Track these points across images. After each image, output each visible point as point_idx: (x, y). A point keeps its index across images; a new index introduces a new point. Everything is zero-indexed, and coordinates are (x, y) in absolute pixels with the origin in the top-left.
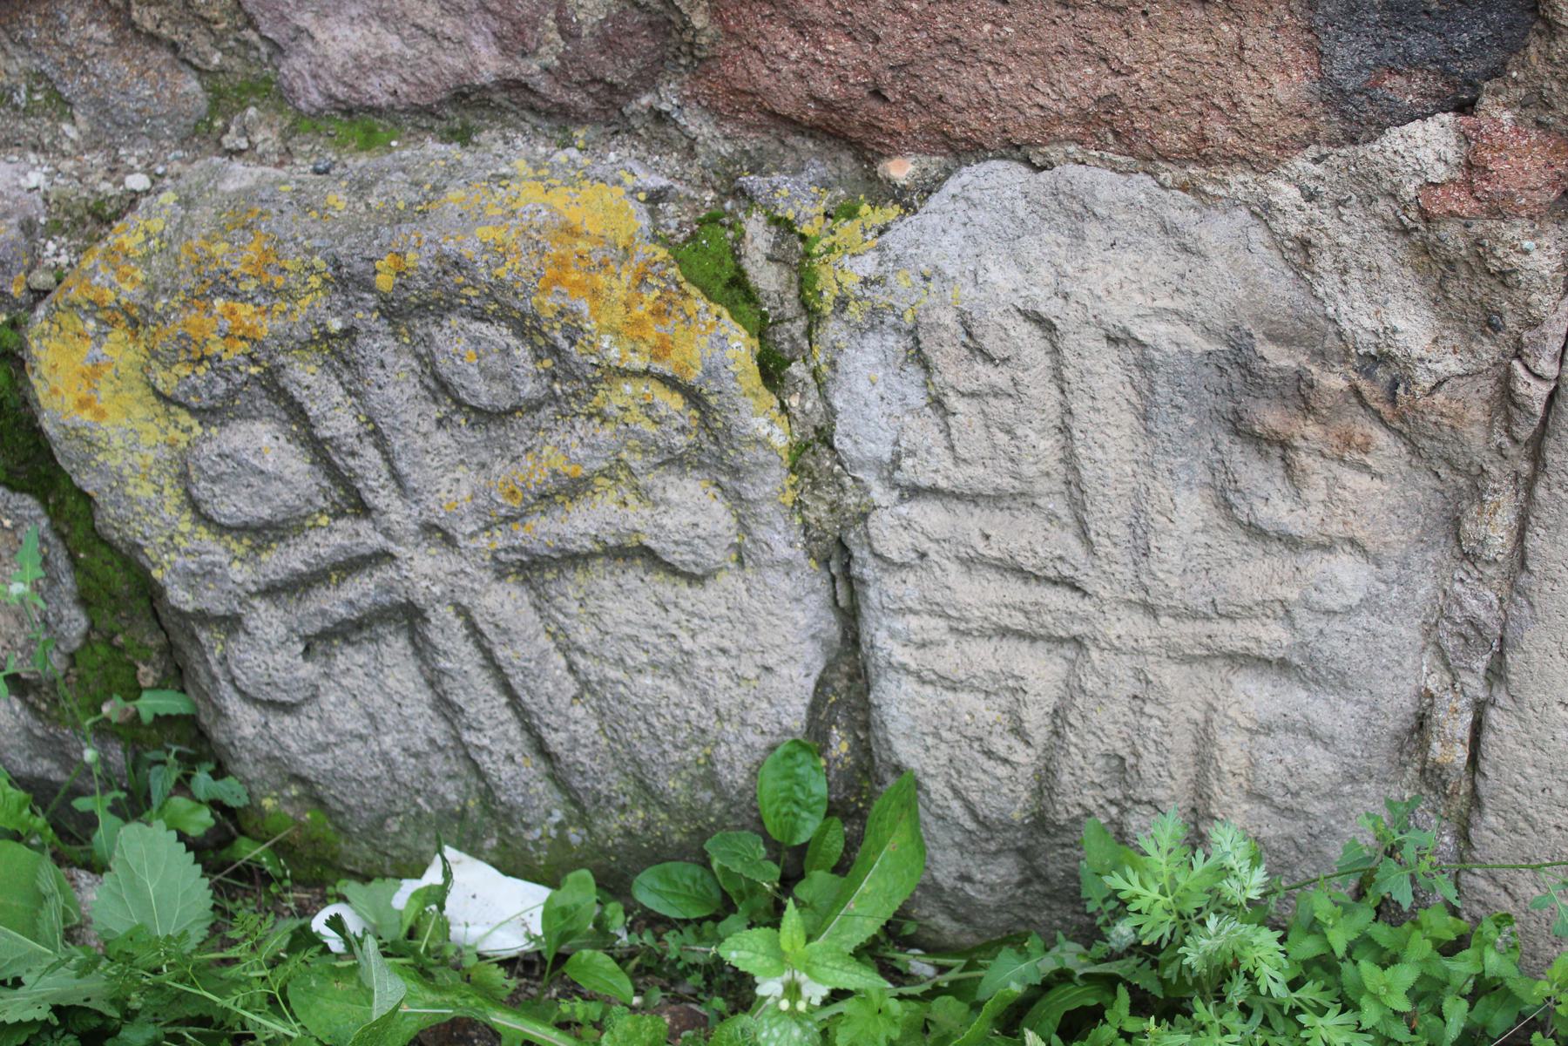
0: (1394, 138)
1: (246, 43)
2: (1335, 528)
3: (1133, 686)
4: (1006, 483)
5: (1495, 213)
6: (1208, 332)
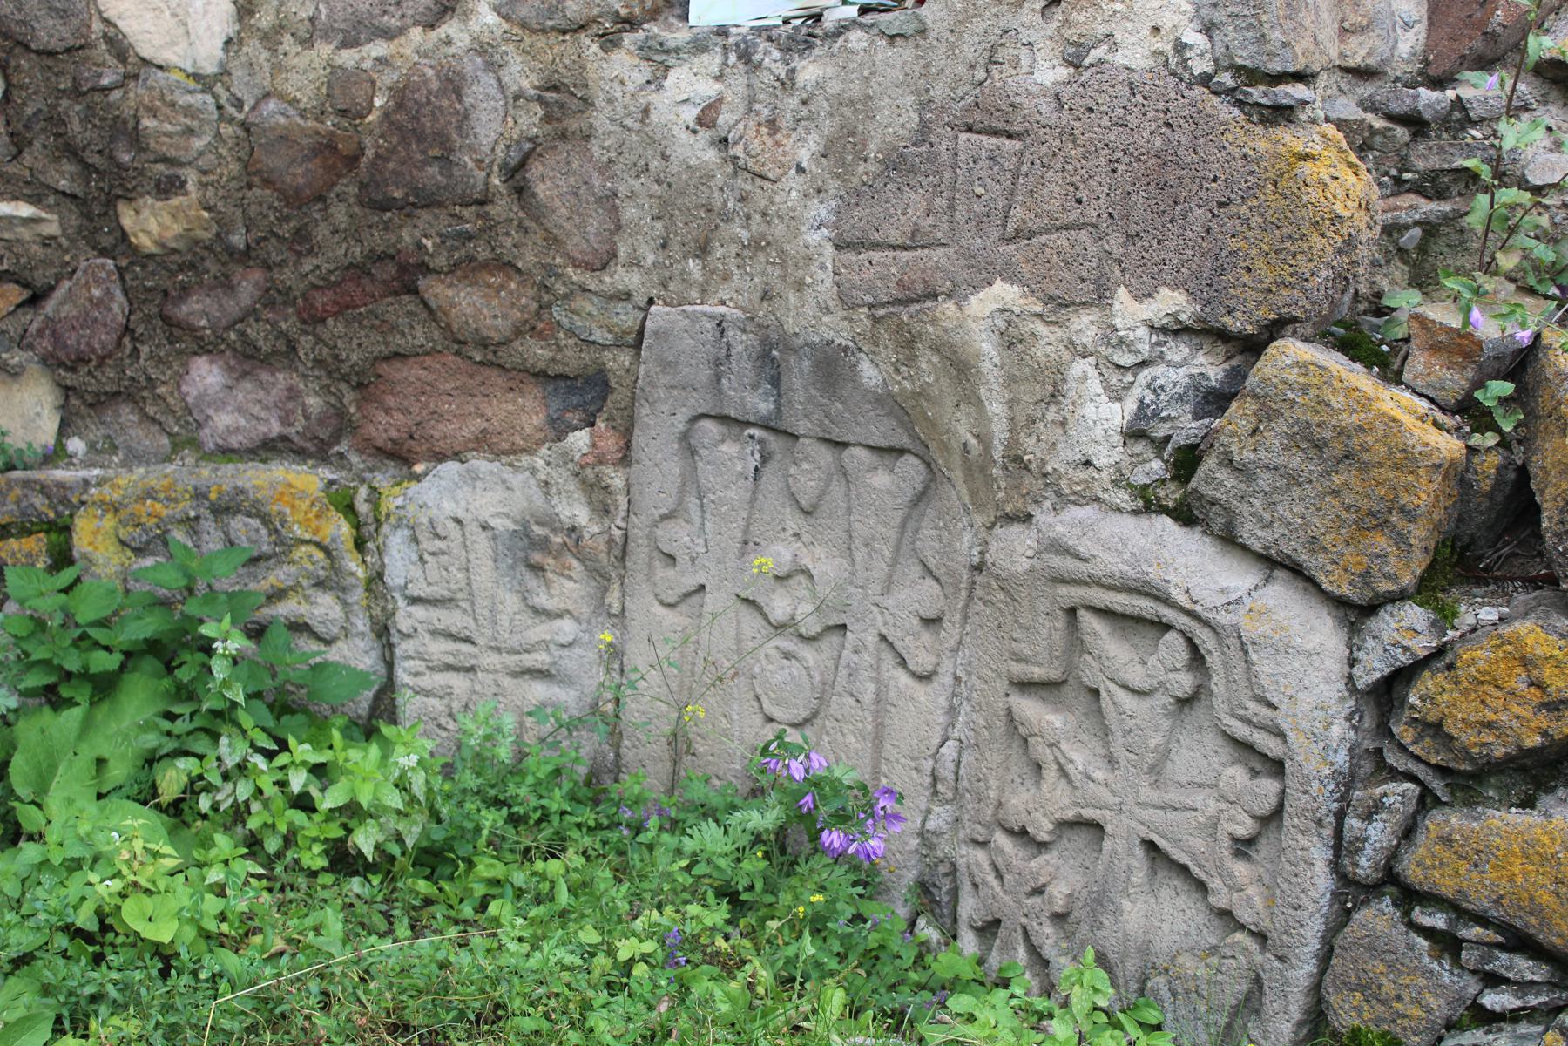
0: (571, 437)
1: (187, 422)
2: (562, 606)
3: (494, 689)
4: (446, 593)
5: (601, 463)
6: (515, 522)
